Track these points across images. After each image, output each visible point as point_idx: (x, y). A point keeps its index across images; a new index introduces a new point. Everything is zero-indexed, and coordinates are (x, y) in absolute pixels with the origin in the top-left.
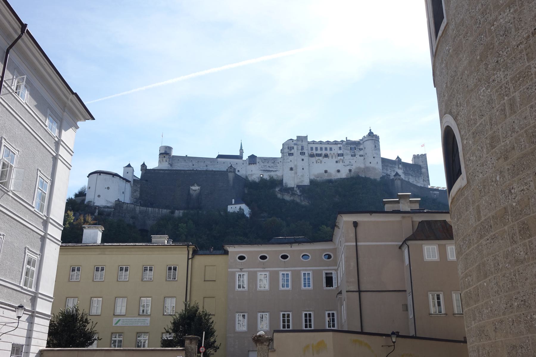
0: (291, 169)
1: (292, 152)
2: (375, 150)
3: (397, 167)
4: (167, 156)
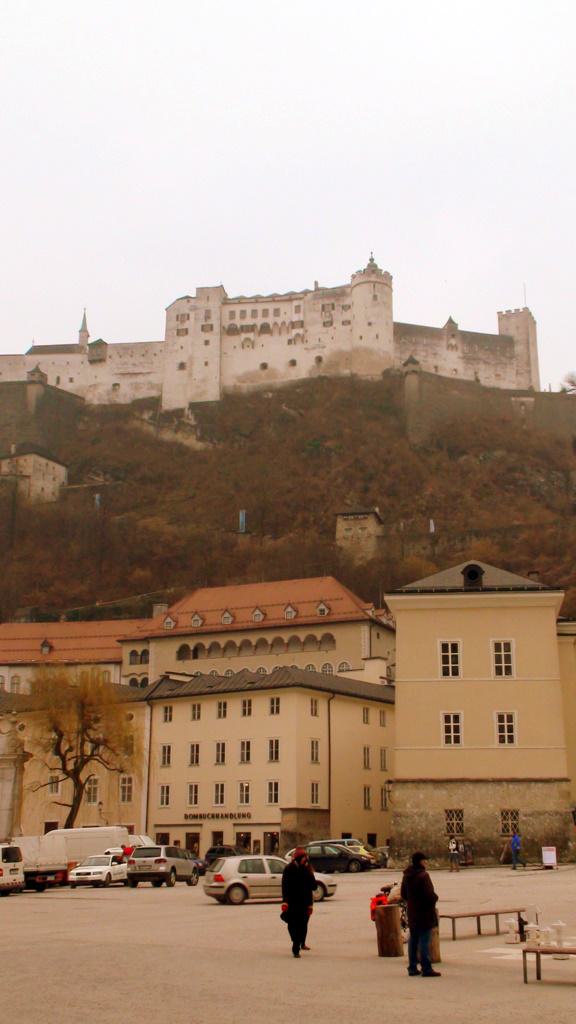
0: (182, 366)
1: (187, 325)
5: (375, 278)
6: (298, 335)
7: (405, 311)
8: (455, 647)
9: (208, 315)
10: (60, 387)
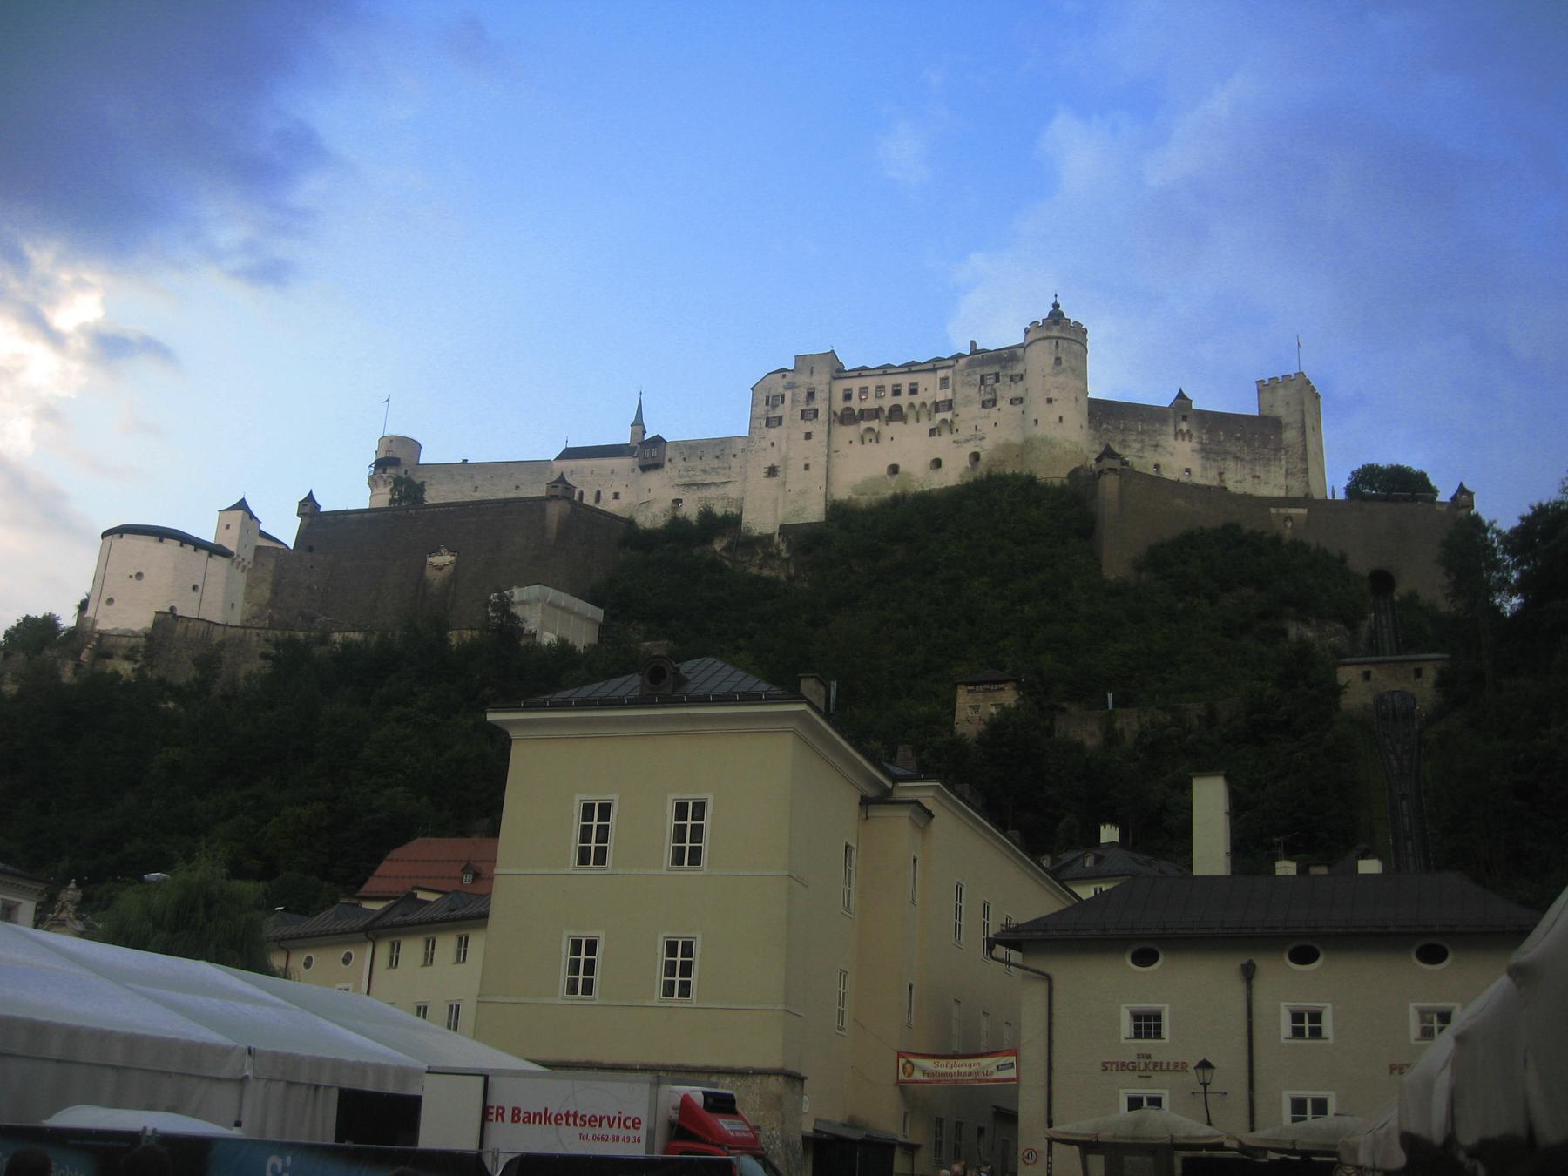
1: (778, 412)
2: (1058, 374)
3: (1171, 429)
4: (391, 471)
5: (1061, 333)
6: (944, 421)
7: (1109, 376)
8: (605, 810)
9: (814, 395)
10: (599, 506)
